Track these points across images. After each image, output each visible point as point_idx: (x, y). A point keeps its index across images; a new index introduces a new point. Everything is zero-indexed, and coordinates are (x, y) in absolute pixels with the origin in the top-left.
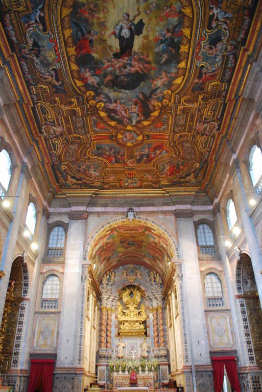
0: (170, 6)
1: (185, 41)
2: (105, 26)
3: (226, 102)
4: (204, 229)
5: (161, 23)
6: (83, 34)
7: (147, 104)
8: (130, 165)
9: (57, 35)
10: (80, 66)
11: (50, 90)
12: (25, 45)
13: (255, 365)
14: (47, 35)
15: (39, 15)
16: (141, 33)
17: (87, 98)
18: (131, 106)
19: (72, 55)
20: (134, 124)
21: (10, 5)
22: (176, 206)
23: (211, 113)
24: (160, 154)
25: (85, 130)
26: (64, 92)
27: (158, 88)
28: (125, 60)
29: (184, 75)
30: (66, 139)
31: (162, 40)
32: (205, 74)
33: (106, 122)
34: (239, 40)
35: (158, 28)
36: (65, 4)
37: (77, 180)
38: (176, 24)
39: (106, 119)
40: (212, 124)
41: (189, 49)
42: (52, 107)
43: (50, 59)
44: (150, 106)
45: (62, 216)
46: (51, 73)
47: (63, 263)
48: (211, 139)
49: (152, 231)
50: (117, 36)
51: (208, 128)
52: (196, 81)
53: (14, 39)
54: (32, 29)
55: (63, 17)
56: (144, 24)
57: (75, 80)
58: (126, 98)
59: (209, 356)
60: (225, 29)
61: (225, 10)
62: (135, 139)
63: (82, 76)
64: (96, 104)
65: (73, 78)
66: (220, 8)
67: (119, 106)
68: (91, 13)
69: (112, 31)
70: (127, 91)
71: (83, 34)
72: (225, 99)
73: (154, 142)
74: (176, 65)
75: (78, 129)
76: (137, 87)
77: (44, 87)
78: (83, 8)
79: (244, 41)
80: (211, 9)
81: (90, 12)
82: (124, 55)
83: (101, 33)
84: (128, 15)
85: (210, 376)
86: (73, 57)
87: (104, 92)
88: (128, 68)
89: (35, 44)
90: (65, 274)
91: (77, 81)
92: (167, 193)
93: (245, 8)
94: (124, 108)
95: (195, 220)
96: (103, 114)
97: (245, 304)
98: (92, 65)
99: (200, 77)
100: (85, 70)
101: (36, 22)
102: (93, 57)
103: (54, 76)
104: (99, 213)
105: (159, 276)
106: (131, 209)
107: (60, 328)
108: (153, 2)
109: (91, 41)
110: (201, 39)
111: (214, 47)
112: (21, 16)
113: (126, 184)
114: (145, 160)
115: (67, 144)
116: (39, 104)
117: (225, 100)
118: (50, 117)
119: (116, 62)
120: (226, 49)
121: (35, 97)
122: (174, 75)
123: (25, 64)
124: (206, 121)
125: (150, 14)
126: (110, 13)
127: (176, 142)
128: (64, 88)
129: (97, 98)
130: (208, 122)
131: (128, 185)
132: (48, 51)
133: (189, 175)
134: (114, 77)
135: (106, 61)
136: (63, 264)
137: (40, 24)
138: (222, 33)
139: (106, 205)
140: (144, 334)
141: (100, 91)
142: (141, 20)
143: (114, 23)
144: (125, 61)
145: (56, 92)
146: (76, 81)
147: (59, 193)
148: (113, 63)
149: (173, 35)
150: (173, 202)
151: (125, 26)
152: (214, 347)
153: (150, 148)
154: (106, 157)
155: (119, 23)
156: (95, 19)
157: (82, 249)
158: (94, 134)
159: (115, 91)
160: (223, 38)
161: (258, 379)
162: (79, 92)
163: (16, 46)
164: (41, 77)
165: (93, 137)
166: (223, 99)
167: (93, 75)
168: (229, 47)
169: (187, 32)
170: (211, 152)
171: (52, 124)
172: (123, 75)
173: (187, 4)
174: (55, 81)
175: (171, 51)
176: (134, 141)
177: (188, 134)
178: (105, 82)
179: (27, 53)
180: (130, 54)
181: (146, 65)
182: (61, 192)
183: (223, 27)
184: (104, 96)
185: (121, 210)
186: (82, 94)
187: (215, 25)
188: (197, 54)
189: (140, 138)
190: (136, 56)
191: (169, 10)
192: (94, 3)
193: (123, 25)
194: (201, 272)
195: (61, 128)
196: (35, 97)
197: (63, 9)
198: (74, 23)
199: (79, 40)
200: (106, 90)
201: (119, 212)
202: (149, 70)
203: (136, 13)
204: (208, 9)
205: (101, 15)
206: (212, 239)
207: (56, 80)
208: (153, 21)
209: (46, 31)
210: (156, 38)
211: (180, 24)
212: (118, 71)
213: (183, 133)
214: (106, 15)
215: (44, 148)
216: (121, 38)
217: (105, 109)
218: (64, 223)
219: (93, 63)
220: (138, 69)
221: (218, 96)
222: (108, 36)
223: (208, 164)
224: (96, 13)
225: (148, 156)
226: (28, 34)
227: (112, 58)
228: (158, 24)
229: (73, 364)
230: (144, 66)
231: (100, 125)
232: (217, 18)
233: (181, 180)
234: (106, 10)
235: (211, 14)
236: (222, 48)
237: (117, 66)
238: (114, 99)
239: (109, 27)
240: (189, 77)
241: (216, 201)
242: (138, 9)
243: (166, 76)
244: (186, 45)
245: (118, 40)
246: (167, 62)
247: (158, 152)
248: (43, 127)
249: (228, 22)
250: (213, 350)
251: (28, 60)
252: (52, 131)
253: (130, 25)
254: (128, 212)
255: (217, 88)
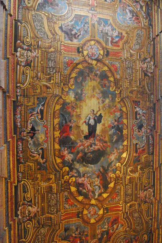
0: (116, 106)
1: (125, 127)
2: (80, 117)
3: (154, 170)
5: (112, 116)
6: (66, 122)
7: (106, 176)
9: (49, 122)
10: (61, 146)
11: (35, 168)
12: (25, 129)
14: (42, 122)
15: (40, 109)
16: (101, 122)
17: (63, 173)
18: (95, 179)
19: (57, 137)
20: (96, 197)
21: (23, 101)
23: (147, 180)
24: (117, 229)
25: (57, 208)
26: (46, 169)
27: (113, 161)
28: (91, 141)
29: (127, 151)
30: (38, 222)
31: (112, 126)
32: (139, 149)
33: (75, 197)
34: (152, 126)
35: (110, 119)
36: (58, 103)
38: (119, 116)
39: (76, 194)
40: (149, 191)
41: (128, 132)
42: (33, 184)
43: (41, 140)
44: (108, 178)
46: (39, 152)
48: (151, 206)
50: (87, 124)
51: (147, 195)
52: (135, 154)
53: (19, 124)
54: (33, 117)
55: (55, 110)
56: (102, 117)
57: (56, 157)
58: (92, 172)
60: (144, 119)
61: (142, 109)
62: (97, 214)
63: (62, 154)
64: (69, 179)
65: (55, 155)
66: (140, 107)
67: (86, 179)
68: (73, 109)
69: (84, 121)
70: (92, 166)
71: (66, 122)
72: (153, 168)
73: (112, 215)
74: (122, 143)
75: (51, 207)
76: (98, 162)
77: (31, 164)
78: (68, 106)
79: (154, 126)
80: (135, 108)
81: (72, 108)
82: (90, 137)
83: (77, 121)
84: (94, 111)
86: (58, 139)
87: (76, 167)
88: (93, 146)
89: (33, 129)
91: (57, 158)
93: (150, 108)
94: (89, 181)
96: (73, 189)
98: (69, 145)
99: (136, 152)
100: (64, 149)
101: (38, 113)
102: (71, 138)
103: (41, 155)
108: (107, 104)
109: (71, 127)
110: (133, 126)
111: (140, 131)
112: (28, 109)
114: (106, 237)
115: (38, 228)
116: (23, 182)
117: (153, 169)
118: (29, 196)
119: (85, 142)
120: (147, 132)
121: (21, 175)
122: (121, 151)
123: (21, 144)
124: (145, 188)
125: (105, 111)
126: (83, 109)
127: (127, 213)
128: (46, 165)
129: (70, 173)
130: (146, 190)
132: (40, 134)
134: (83, 154)
135: (79, 141)
137: (40, 115)
138: (143, 122)
141: (73, 166)
142: (101, 114)
143: (85, 115)
144: (91, 141)
145: (39, 169)
146: (57, 158)
148: (83, 143)
149: (118, 123)
151: (92, 117)
153: (109, 223)
154: (72, 239)
155: (88, 115)
156: (75, 112)
158: (64, 212)
159: (84, 166)
160: (144, 125)
162: (57, 168)
163: (18, 129)
164: (31, 155)
165: (64, 216)
166: (152, 168)
167: (69, 153)
168: (148, 130)
169: (125, 121)
170: (153, 220)
171: (29, 204)
172: (89, 152)
173: (123, 105)
174: (40, 159)
175: (118, 134)
176: (96, 216)
177: (136, 203)
178: (77, 159)
179: (25, 135)
180: (94, 136)
181: (104, 144)
183: (143, 118)
184: (75, 171)
186: (60, 170)
187: (139, 117)
188: (132, 135)
189: (101, 212)
190: (98, 138)
191: (115, 108)
192: (75, 103)
193: (90, 116)
195: (36, 208)
196: (21, 175)
197: (56, 105)
198: (62, 114)
199: (63, 126)
200: (77, 166)
202: (106, 148)
203: (98, 109)
204: (134, 108)
205: (78, 110)
207: (41, 158)
208: (107, 114)
209: (42, 120)
210: (109, 125)
211: (121, 116)
212: (86, 149)
213: (132, 203)
214: (81, 110)
215: (15, 236)
216: (89, 125)
217: (75, 184)
219: (70, 143)
220: (100, 147)
221: (149, 166)
222: (82, 124)
223: (153, 234)
224: (75, 109)
225: (107, 232)
226: (29, 121)
227: (83, 139)
228: (109, 117)
230: (103, 145)
231: (70, 201)
232: (139, 113)
234: (81, 107)
235: (136, 111)
236: (145, 131)
237: (86, 145)
238: (82, 173)
239: (82, 118)
240: (130, 152)
242: (99, 107)
243: (117, 152)
244: (126, 129)
245: (87, 126)
246: (117, 141)
247: (115, 226)
248: (20, 208)
249: (145, 115)
251: (24, 141)
252: (27, 212)
253: (95, 117)
255: (147, 159)
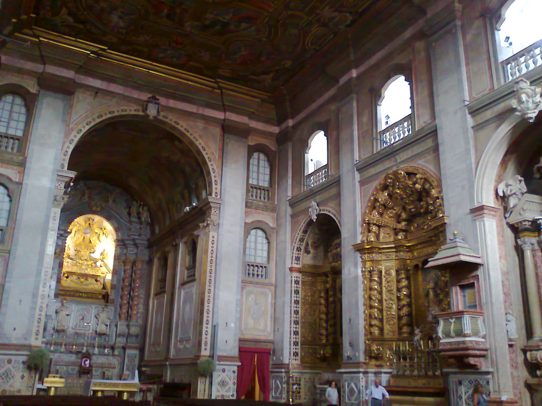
4: (259, 160)
8: (188, 29)
13: (298, 362)
22: (228, 114)
24: (245, 29)
37: (78, 21)
40: (346, 16)
45: (25, 77)
47: (22, 165)
49: (176, 142)
59: (237, 344)
85: (234, 372)
90: (24, 186)
92: (220, 88)
95: (250, 144)
97: (300, 282)
104: (97, 92)
105: (149, 210)
106: (154, 98)
107: (7, 279)
113: (162, 55)
131: (164, 58)
133: (267, 73)
136: (21, 169)
139: (111, 80)
140: (100, 297)
147: (27, 31)
150: (224, 105)
152: (245, 332)
157: (61, 148)
161: (300, 381)
182: (31, 29)
185: (135, 94)
194: (246, 223)
201: (133, 98)
206: (267, 178)
218: (28, 92)
229: (26, 339)
233: (251, 77)
241: (290, 123)
247: (244, 25)
250: (242, 337)
254: (149, 102)
